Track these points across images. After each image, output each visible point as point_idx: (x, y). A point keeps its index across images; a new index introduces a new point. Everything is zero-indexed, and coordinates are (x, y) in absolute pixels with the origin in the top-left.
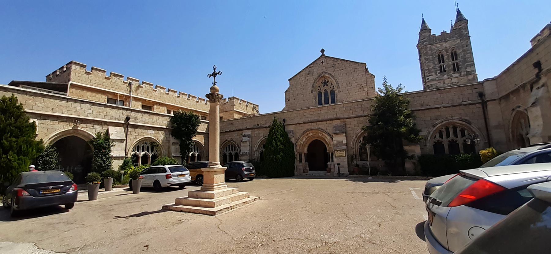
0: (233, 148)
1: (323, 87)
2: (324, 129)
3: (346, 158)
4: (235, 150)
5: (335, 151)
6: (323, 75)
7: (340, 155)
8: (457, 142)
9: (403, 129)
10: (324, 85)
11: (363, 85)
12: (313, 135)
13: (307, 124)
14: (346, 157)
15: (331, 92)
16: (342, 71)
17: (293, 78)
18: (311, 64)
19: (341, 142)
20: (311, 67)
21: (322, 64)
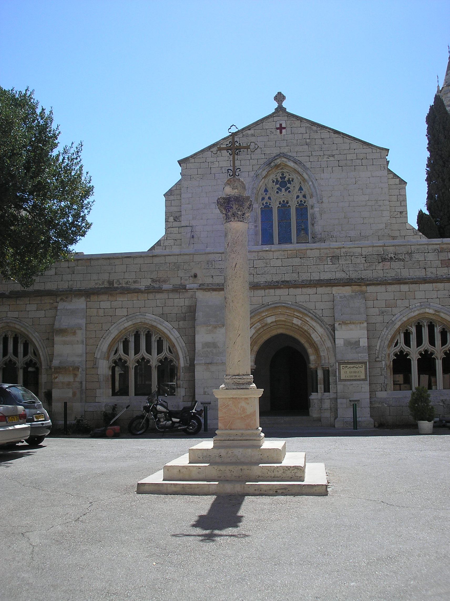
0: (21, 348)
1: (277, 192)
2: (311, 306)
3: (368, 382)
4: (25, 353)
5: (340, 364)
6: (278, 161)
12: (276, 321)
14: (365, 380)
15: (297, 209)
16: (331, 159)
17: (192, 156)
20: (247, 136)
21: (279, 130)
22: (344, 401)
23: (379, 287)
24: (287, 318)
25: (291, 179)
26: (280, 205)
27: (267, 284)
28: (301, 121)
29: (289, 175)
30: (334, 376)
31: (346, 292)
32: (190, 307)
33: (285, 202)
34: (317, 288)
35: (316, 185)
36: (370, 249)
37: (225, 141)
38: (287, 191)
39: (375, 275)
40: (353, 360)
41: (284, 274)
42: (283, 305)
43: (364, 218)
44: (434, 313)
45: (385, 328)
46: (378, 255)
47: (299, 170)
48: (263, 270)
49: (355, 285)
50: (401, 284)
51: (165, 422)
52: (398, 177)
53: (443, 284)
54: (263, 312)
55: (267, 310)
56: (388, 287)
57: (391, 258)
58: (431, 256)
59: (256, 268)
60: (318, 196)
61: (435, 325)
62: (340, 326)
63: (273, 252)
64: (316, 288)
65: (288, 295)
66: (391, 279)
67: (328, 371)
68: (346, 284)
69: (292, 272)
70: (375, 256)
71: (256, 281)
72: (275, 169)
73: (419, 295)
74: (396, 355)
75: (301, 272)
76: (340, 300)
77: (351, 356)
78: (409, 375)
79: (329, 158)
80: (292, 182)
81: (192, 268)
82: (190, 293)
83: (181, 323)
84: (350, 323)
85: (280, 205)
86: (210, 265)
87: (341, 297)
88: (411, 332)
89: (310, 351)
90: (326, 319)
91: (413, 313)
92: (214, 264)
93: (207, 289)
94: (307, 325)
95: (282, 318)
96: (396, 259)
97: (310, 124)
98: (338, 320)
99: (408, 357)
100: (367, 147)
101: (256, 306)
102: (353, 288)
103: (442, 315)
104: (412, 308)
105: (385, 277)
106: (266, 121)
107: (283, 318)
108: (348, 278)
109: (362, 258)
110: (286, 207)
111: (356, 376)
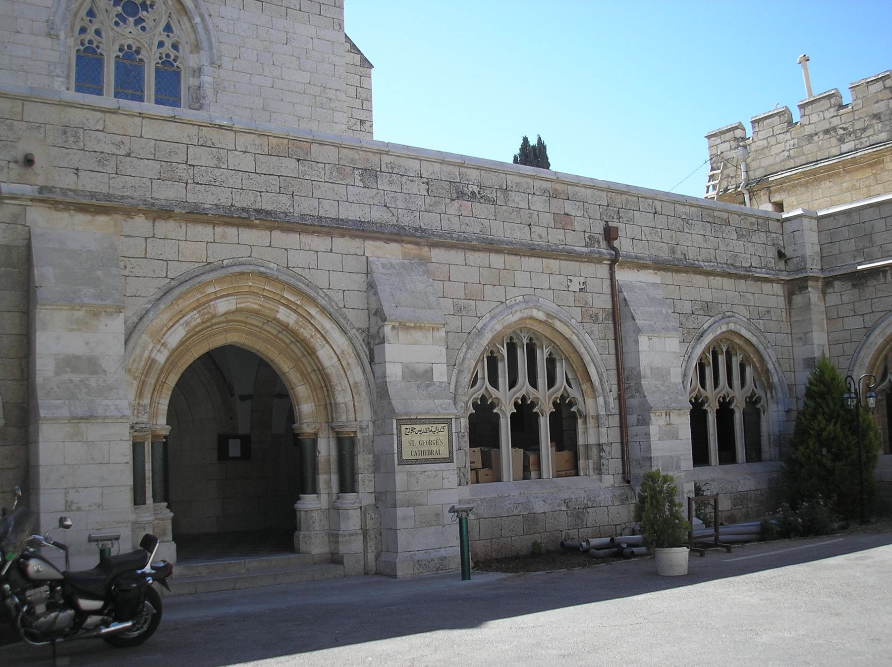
2: (320, 279)
5: (400, 422)
7: (423, 453)
8: (758, 406)
9: (487, 348)
12: (237, 311)
13: (204, 232)
14: (450, 460)
15: (158, 71)
19: (426, 372)
22: (410, 511)
23: (453, 252)
24: (264, 304)
26: (121, 54)
27: (221, 212)
30: (370, 453)
33: (134, 49)
35: (210, 26)
36: (437, 167)
38: (140, 26)
39: (446, 226)
40: (428, 413)
41: (259, 193)
42: (262, 269)
43: (301, 118)
44: (545, 318)
45: (464, 345)
46: (450, 182)
48: (210, 175)
49: (410, 243)
50: (490, 251)
51: (53, 615)
52: (359, 52)
53: (558, 261)
54: (210, 283)
55: (220, 280)
57: (473, 193)
58: (539, 203)
59: (193, 166)
60: (215, 51)
61: (538, 344)
62: (395, 332)
63: (235, 132)
64: (330, 239)
65: (270, 246)
66: (474, 238)
67: (353, 441)
68: (392, 237)
70: (446, 185)
71: (192, 199)
73: (522, 279)
74: (475, 405)
76: (384, 271)
77: (420, 405)
78: (493, 451)
80: (150, 10)
81: (19, 139)
84: (415, 327)
85: (121, 54)
86: (72, 139)
87: (384, 266)
88: (499, 358)
89: (302, 391)
90: (351, 315)
92: (81, 137)
94: (310, 325)
95: (252, 304)
96: (482, 197)
98: (393, 318)
99: (495, 411)
101: (192, 266)
102: (405, 248)
103: (558, 325)
104: (512, 306)
105: (464, 232)
108: (396, 224)
109: (421, 184)
110: (134, 60)
111: (431, 452)
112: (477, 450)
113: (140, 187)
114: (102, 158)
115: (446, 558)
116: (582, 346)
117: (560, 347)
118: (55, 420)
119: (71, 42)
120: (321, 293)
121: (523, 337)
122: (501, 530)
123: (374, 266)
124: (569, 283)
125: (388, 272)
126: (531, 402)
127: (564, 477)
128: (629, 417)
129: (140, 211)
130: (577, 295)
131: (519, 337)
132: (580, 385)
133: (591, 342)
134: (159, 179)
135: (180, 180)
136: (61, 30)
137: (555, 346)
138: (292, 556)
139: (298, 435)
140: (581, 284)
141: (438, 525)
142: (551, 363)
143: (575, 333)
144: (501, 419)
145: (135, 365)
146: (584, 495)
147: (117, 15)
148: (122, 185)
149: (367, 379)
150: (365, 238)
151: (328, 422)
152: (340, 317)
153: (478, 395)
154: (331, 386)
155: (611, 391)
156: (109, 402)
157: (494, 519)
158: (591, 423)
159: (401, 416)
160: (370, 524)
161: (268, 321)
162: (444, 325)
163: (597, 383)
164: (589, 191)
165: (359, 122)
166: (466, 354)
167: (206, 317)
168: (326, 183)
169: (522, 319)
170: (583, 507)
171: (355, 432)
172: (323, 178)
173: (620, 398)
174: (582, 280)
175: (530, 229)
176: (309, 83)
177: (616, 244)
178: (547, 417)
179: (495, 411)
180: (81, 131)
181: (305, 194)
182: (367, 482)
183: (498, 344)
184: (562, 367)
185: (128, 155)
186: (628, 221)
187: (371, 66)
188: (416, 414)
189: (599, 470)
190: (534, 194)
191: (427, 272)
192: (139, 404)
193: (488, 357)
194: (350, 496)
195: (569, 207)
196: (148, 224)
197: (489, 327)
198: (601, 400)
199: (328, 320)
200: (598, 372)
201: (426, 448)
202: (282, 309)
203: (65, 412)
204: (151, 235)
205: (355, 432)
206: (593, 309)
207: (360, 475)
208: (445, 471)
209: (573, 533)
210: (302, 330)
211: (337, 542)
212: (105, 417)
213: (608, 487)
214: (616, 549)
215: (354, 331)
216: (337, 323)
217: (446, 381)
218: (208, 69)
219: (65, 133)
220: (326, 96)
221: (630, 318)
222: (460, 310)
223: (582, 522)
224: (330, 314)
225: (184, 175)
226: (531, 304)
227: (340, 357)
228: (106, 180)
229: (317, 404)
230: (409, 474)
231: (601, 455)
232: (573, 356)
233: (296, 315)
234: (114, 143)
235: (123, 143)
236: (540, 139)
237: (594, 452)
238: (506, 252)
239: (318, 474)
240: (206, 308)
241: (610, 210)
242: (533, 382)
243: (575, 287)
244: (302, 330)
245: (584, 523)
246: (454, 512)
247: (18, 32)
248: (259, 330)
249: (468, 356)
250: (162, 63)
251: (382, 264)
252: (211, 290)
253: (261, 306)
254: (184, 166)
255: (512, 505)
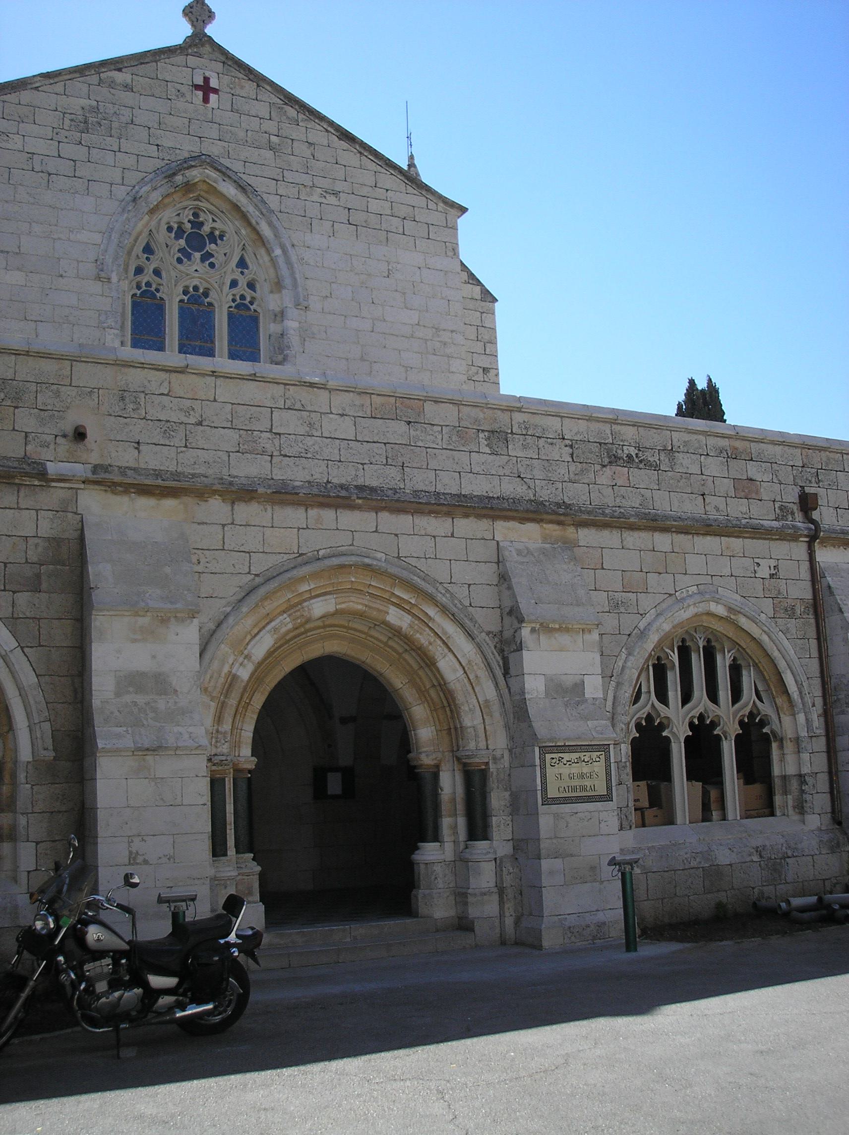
2: (439, 571)
5: (544, 750)
6: (195, 174)
7: (574, 789)
9: (653, 653)
10: (186, 254)
11: (445, 337)
12: (337, 613)
13: (295, 516)
14: (608, 798)
15: (230, 316)
16: (332, 199)
18: (117, 64)
20: (112, 84)
21: (200, 94)
22: (558, 863)
23: (606, 533)
24: (371, 604)
25: (217, 233)
26: (186, 298)
27: (315, 491)
28: (258, 86)
29: (214, 221)
30: (506, 790)
31: (529, 539)
32: (55, 542)
33: (201, 291)
34: (453, 518)
35: (294, 259)
37: (47, 82)
38: (207, 262)
40: (579, 738)
41: (361, 466)
42: (367, 561)
43: (409, 369)
44: (726, 614)
45: (623, 650)
46: (600, 444)
47: (250, 209)
48: (300, 445)
50: (655, 529)
51: (117, 994)
52: (478, 283)
54: (302, 579)
55: (314, 576)
56: (626, 534)
57: (629, 456)
58: (714, 466)
59: (279, 434)
60: (300, 289)
62: (535, 636)
63: (330, 391)
64: (451, 520)
65: (376, 531)
66: (633, 513)
67: (484, 774)
68: (531, 516)
69: (385, 462)
70: (595, 448)
71: (278, 475)
72: (180, 194)
73: (695, 563)
74: (638, 726)
75: (409, 465)
76: (520, 559)
78: (663, 785)
79: (325, 197)
80: (219, 242)
81: (68, 408)
82: (57, 494)
83: (23, 598)
84: (560, 629)
85: (186, 298)
86: (132, 406)
87: (519, 552)
91: (683, 611)
93: (120, 484)
94: (427, 629)
95: (356, 604)
96: (641, 461)
97: (282, 97)
98: (533, 618)
99: (664, 734)
100: (415, 192)
101: (280, 558)
102: (545, 529)
103: (743, 622)
104: (683, 599)
105: (619, 507)
106: (167, 60)
107: (358, 603)
108: (533, 498)
110: (202, 304)
111: (584, 788)
112: (643, 784)
113: (215, 462)
114: (168, 428)
115: (604, 923)
116: (775, 648)
117: (748, 651)
118: (116, 752)
119: (125, 285)
120: (440, 588)
121: (698, 639)
122: (675, 887)
123: (507, 553)
124: (756, 568)
125: (525, 560)
126: (712, 722)
127: (755, 817)
128: (838, 739)
129: (215, 492)
130: (767, 582)
131: (693, 638)
132: (774, 698)
133: (786, 643)
134: (238, 452)
135: (263, 453)
136: (112, 271)
137: (740, 649)
138: (408, 921)
139: (415, 767)
140: (772, 568)
141: (595, 881)
142: (735, 670)
143: (765, 632)
144: (673, 744)
145: (212, 684)
146: (782, 841)
147: (179, 251)
148: (192, 461)
149: (501, 696)
150: (494, 518)
151: (453, 751)
152: (465, 619)
153: (643, 714)
154: (455, 705)
155: (814, 705)
156: (180, 729)
157: (666, 874)
158: (789, 747)
159: (545, 742)
160: (508, 881)
161: (375, 625)
162: (598, 625)
163: (795, 696)
164: (778, 449)
165: (481, 370)
166: (625, 662)
167: (299, 621)
168: (444, 451)
169: (696, 615)
170: (780, 855)
171: (487, 764)
172: (440, 443)
173: (827, 715)
174: (773, 563)
175: (704, 499)
176: (418, 324)
177: (815, 515)
178: (731, 740)
179: (664, 734)
180: (143, 395)
181: (419, 465)
182: (502, 826)
183: (667, 648)
184: (750, 676)
185: (200, 424)
186: (830, 485)
187: (495, 300)
188: (564, 740)
189: (801, 808)
190: (708, 454)
191: (574, 559)
192: (217, 731)
193: (654, 666)
194: (482, 845)
195: (753, 470)
196: (226, 508)
197: (655, 626)
198: (801, 718)
199: (452, 623)
200: (796, 681)
201: (576, 783)
202: (392, 610)
203: (128, 742)
204: (230, 521)
205: (487, 764)
206: (788, 601)
207: (494, 818)
208: (602, 811)
209: (769, 890)
210: (418, 635)
211: (466, 904)
212: (177, 748)
213: (813, 831)
214: (824, 912)
215: (483, 634)
216: (462, 626)
217: (602, 696)
218: (292, 312)
219: (123, 399)
220: (438, 339)
221: (837, 609)
222: (617, 606)
223: (780, 876)
224: (453, 615)
225: (269, 447)
226: (707, 596)
227: (466, 669)
228: (173, 455)
229: (438, 728)
230: (557, 816)
231: (803, 788)
232: (764, 664)
233: (410, 617)
234: (181, 410)
235: (193, 409)
236: (710, 380)
237: (794, 785)
238: (674, 530)
239: (441, 817)
240: (299, 610)
241: (806, 471)
242: (713, 696)
243: (764, 572)
244: (418, 635)
245: (783, 877)
246: (615, 864)
247: (61, 276)
248: (364, 636)
249: (629, 664)
250: (236, 307)
251: (517, 550)
252: (304, 587)
253: (366, 606)
254: (268, 435)
255: (688, 855)
